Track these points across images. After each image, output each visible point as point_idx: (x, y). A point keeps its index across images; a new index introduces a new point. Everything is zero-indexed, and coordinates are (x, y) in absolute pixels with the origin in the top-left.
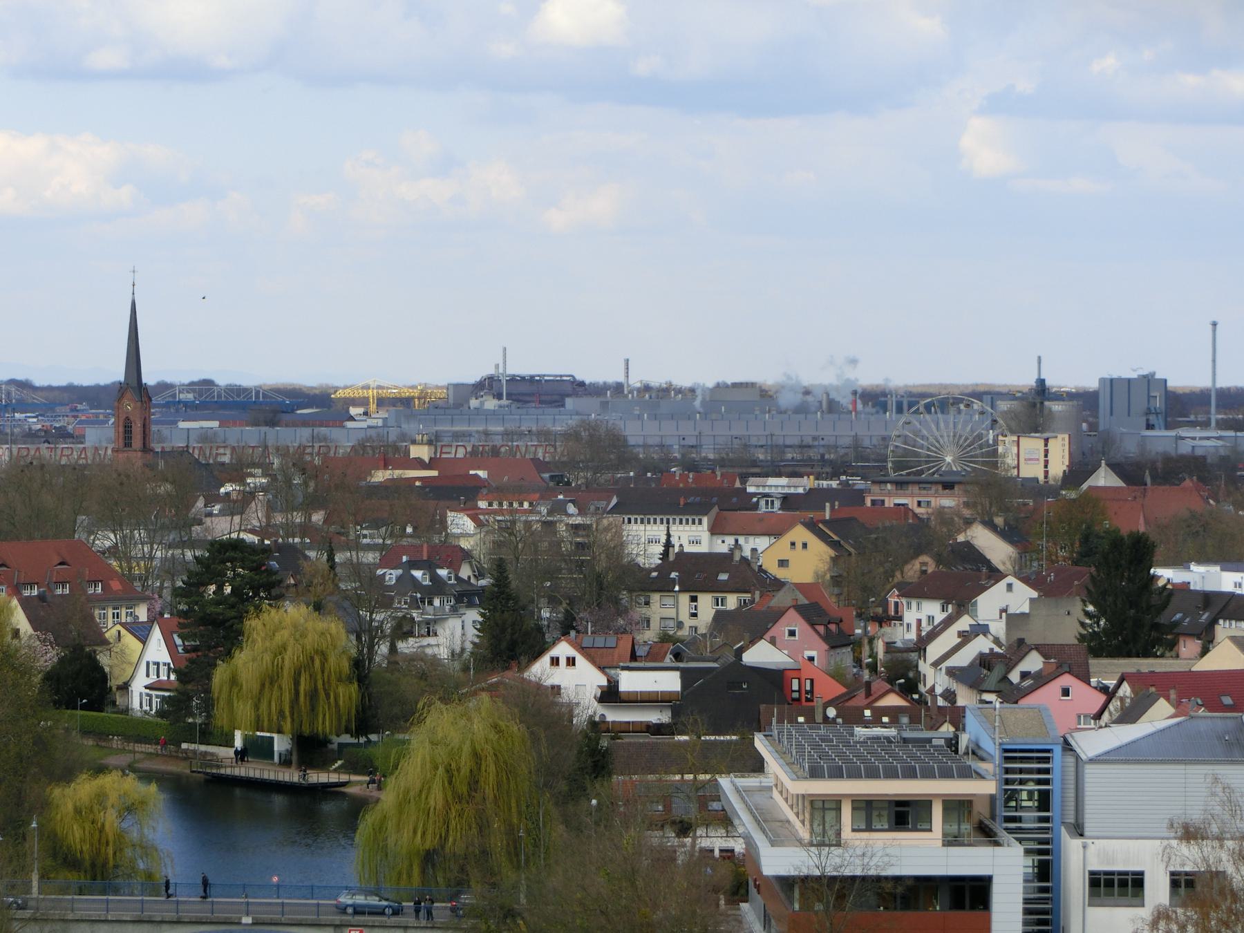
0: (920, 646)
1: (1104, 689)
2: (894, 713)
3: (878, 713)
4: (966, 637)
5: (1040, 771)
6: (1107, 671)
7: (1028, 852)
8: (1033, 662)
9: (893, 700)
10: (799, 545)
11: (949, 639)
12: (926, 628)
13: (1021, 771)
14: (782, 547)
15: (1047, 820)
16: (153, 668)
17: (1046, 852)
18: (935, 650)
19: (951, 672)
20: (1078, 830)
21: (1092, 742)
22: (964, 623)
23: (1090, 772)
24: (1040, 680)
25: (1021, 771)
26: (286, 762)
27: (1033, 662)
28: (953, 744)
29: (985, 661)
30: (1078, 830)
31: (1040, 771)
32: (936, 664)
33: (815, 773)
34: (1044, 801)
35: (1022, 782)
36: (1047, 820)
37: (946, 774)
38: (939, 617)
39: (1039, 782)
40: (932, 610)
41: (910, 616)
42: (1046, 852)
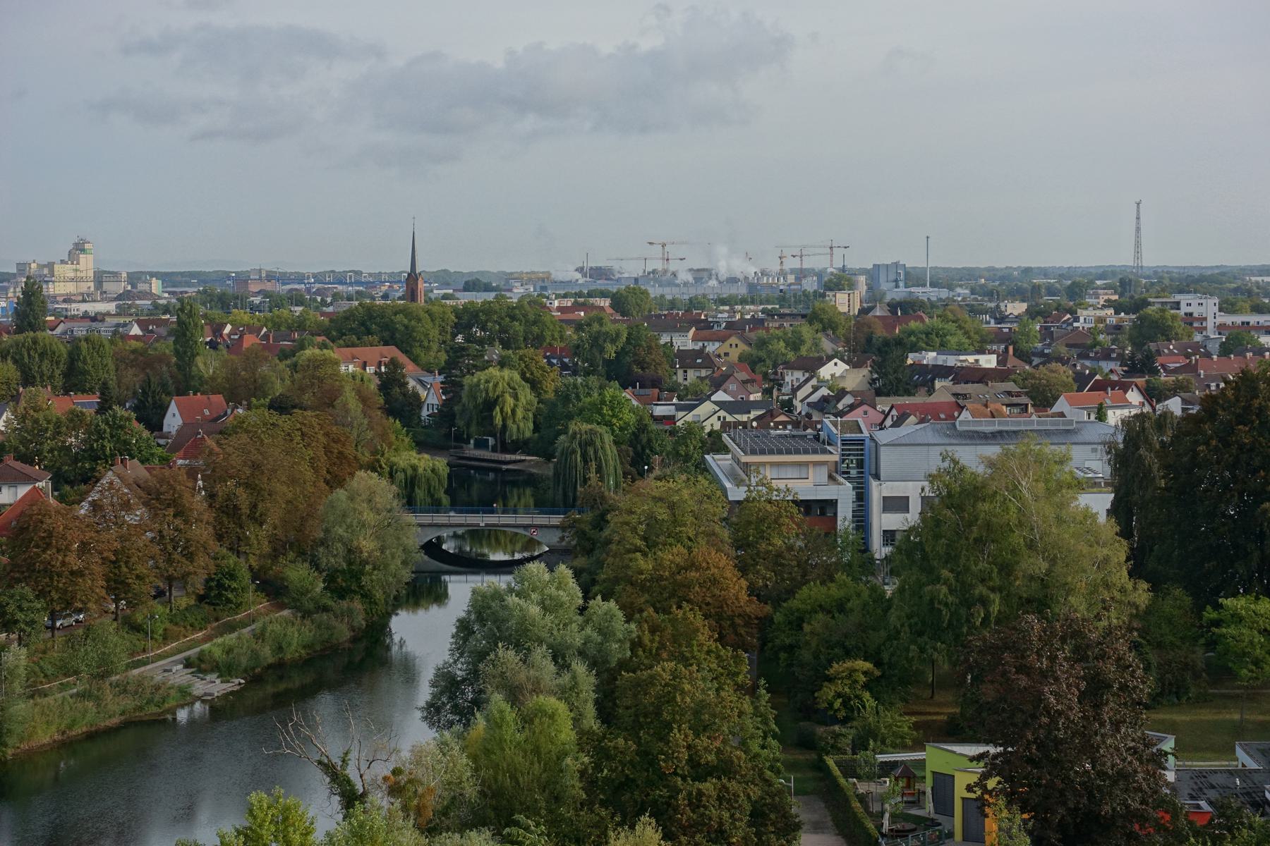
0: (795, 391)
1: (883, 412)
2: (784, 424)
3: (777, 424)
4: (816, 389)
5: (857, 450)
6: (883, 404)
7: (854, 488)
8: (848, 400)
9: (782, 418)
10: (734, 346)
11: (807, 389)
12: (796, 384)
13: (849, 450)
14: (725, 347)
15: (862, 473)
16: (430, 407)
17: (862, 488)
18: (801, 394)
19: (809, 404)
20: (877, 477)
21: (883, 437)
22: (814, 382)
23: (882, 449)
24: (852, 407)
25: (849, 450)
26: (494, 450)
27: (848, 400)
28: (817, 438)
29: (825, 399)
30: (877, 477)
31: (857, 450)
32: (802, 401)
33: (753, 452)
34: (860, 464)
35: (849, 455)
36: (862, 473)
37: (815, 452)
38: (802, 379)
39: (857, 455)
40: (799, 375)
41: (788, 379)
42: (862, 488)
